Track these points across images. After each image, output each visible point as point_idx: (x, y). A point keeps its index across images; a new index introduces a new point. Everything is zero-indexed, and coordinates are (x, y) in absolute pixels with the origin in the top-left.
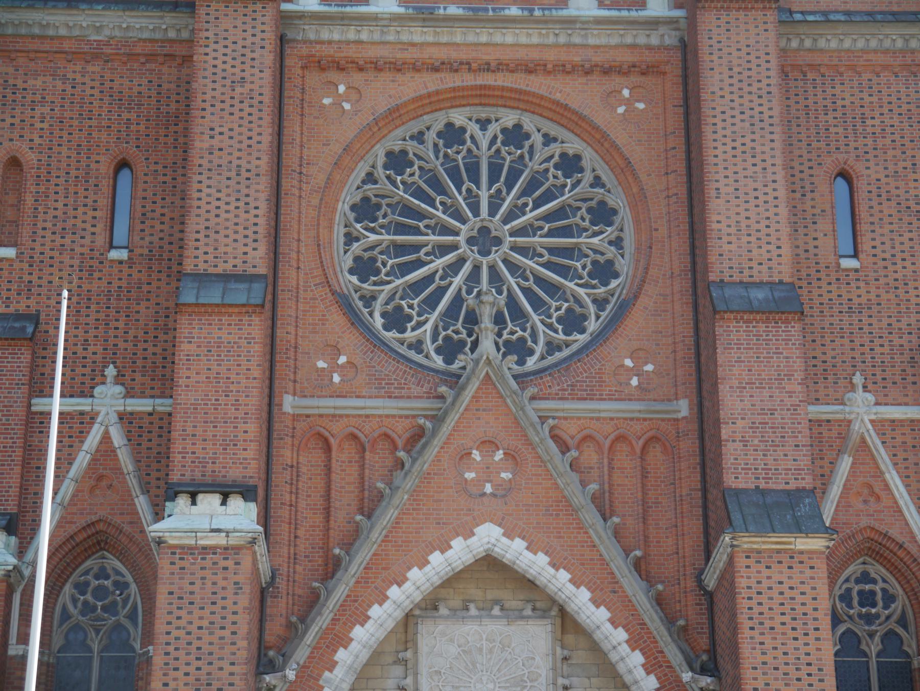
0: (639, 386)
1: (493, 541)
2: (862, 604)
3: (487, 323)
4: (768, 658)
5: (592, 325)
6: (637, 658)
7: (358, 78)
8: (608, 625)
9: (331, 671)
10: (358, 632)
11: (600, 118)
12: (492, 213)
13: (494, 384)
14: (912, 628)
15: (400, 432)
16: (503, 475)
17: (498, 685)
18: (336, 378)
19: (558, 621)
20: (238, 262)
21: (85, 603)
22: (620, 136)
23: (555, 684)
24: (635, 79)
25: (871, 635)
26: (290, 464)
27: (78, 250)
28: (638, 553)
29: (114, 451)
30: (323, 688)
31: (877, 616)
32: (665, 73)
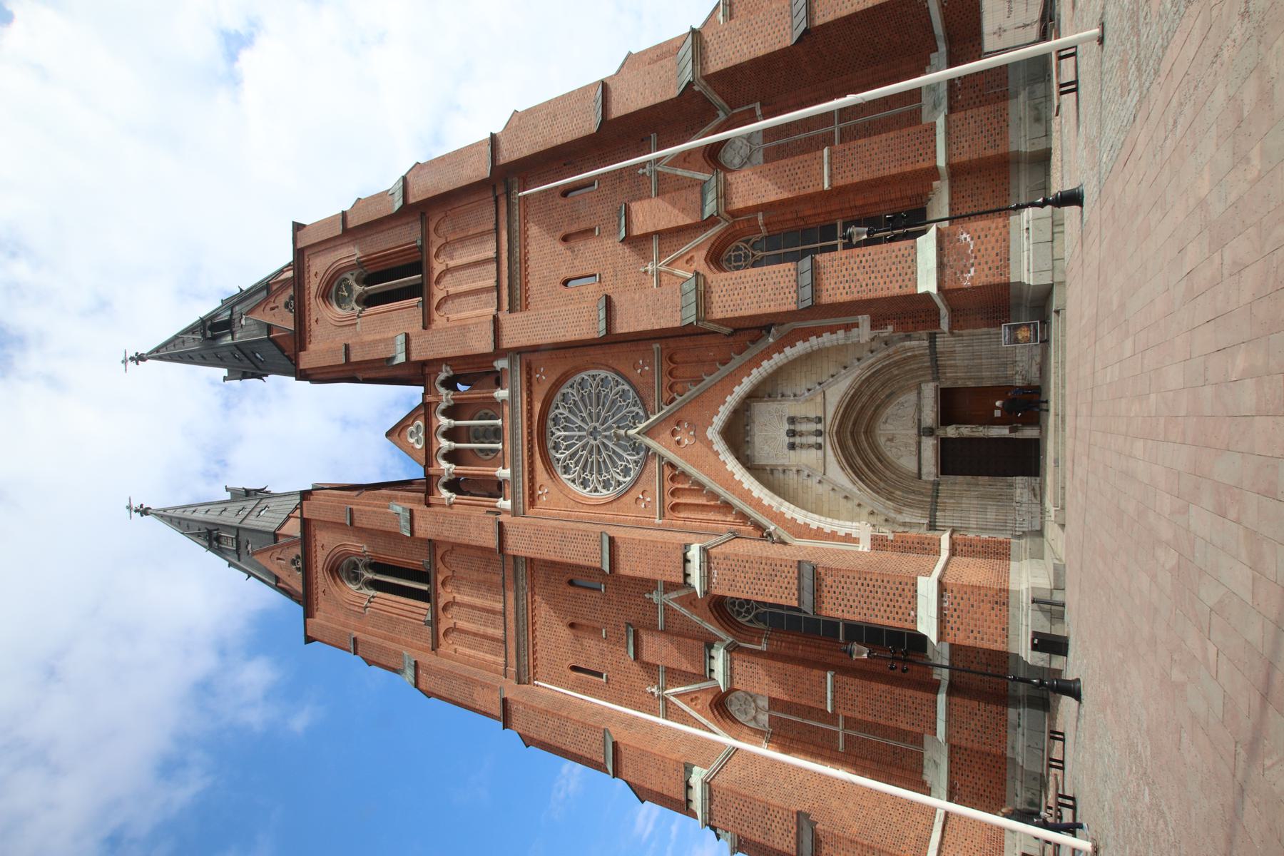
2: (741, 260)
3: (622, 432)
4: (755, 301)
6: (765, 363)
7: (537, 486)
8: (750, 377)
11: (547, 386)
12: (585, 430)
14: (750, 237)
18: (648, 499)
19: (752, 399)
20: (596, 543)
21: (745, 612)
22: (554, 378)
23: (780, 401)
24: (533, 373)
25: (753, 255)
27: (601, 604)
29: (680, 597)
31: (745, 253)
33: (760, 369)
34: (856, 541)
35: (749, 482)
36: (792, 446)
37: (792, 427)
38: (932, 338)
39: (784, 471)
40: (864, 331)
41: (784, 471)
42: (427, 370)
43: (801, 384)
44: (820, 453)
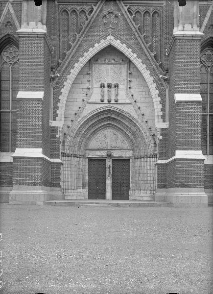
34: (54, 120)
35: (84, 60)
36: (102, 86)
37: (113, 86)
38: (155, 156)
40: (161, 125)
43: (137, 91)
44: (99, 101)
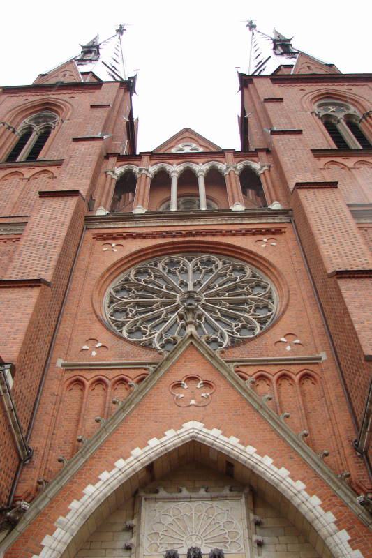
0: (292, 350)
1: (196, 431)
5: (258, 331)
6: (315, 501)
7: (121, 242)
8: (289, 480)
9: (64, 516)
10: (90, 489)
13: (197, 349)
15: (133, 377)
16: (203, 395)
17: (204, 542)
18: (94, 353)
19: (250, 498)
23: (250, 538)
26: (56, 394)
28: (305, 432)
30: (56, 528)
32: (285, 232)
33: (304, 493)
39: (128, 548)
41: (128, 548)
42: (262, 155)
